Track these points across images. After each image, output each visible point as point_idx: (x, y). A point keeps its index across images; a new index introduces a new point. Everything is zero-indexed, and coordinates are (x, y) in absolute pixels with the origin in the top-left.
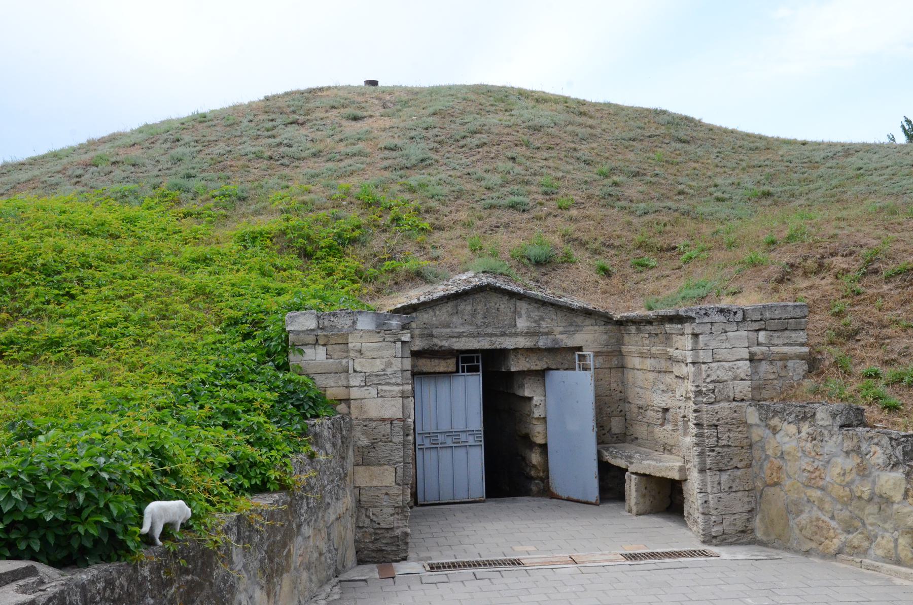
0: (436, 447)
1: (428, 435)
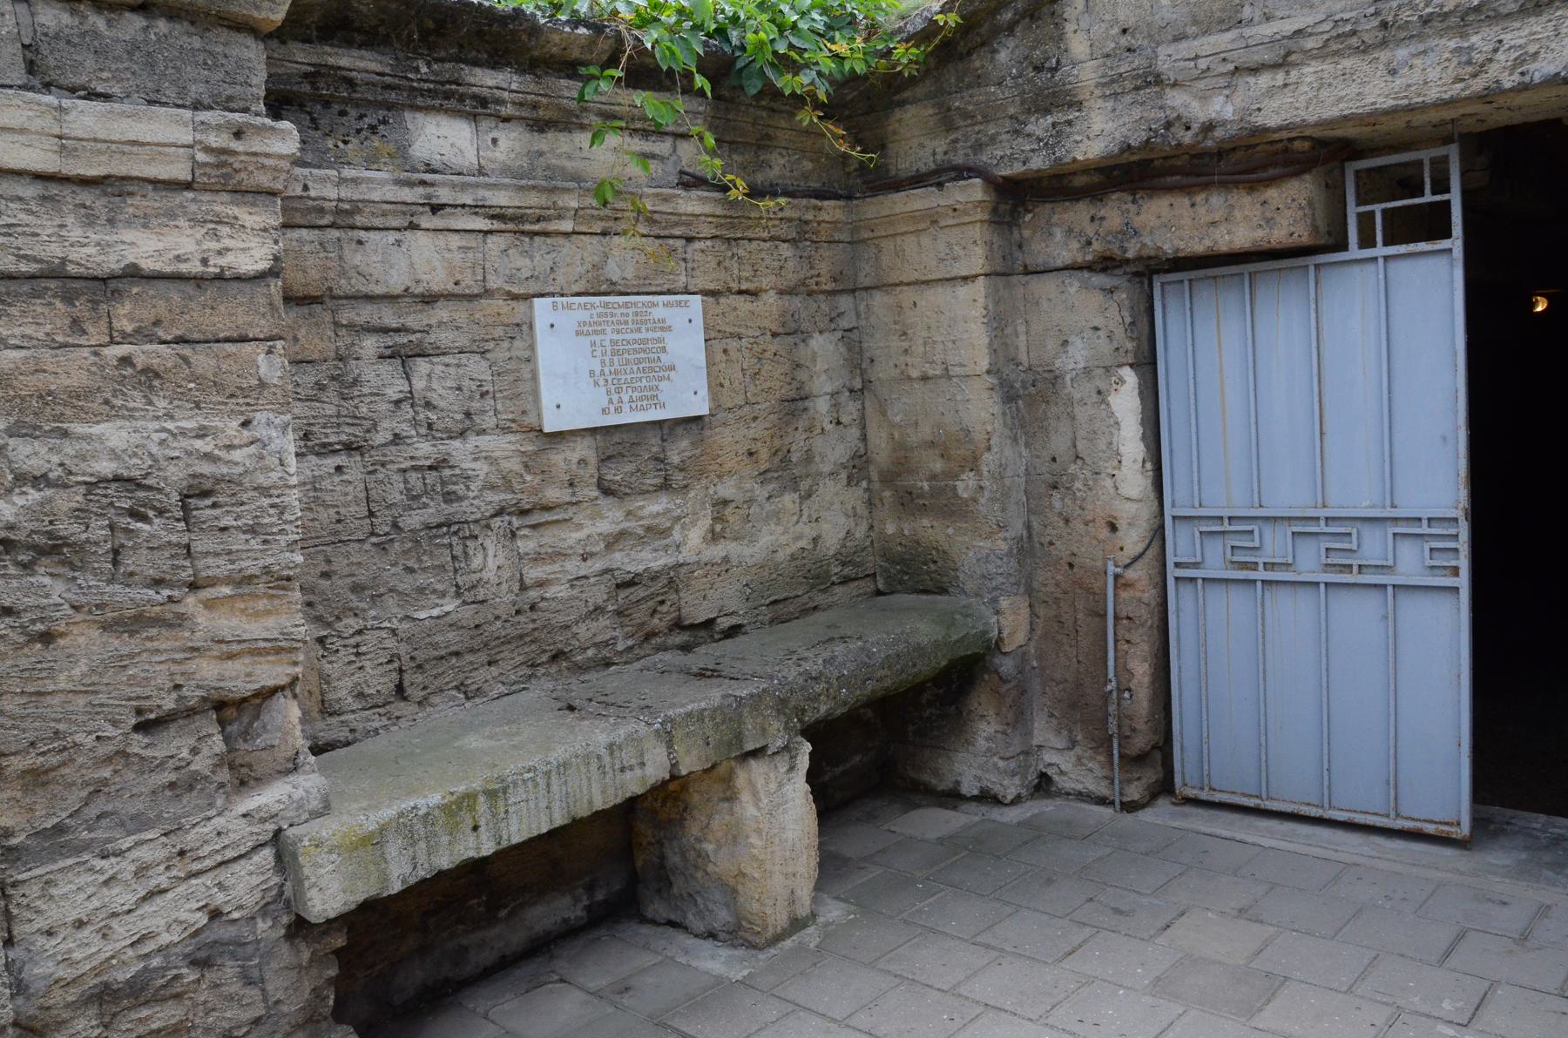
0: (1255, 579)
1: (1216, 527)
